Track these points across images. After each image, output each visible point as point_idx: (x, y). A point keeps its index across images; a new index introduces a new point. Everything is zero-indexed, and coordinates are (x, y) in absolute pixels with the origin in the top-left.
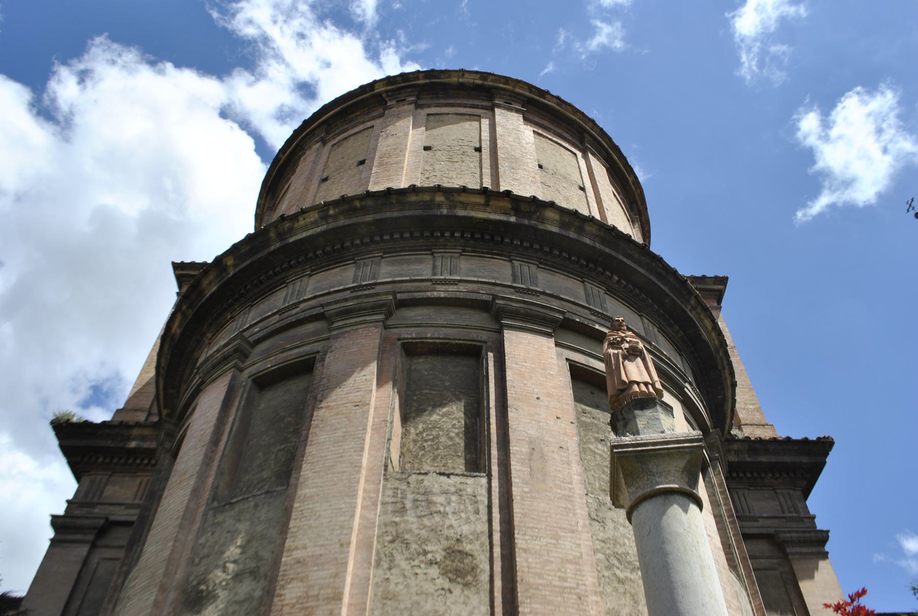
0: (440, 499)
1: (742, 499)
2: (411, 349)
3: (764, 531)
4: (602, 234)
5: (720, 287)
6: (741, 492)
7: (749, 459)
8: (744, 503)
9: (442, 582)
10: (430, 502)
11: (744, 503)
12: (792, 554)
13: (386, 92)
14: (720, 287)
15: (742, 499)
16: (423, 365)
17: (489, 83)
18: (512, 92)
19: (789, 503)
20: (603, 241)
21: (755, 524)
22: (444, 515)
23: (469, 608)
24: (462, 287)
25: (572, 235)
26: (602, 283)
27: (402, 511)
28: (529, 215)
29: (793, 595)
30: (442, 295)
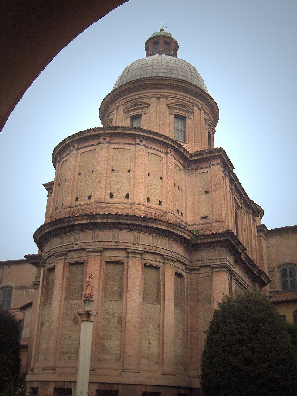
0: (73, 306)
2: (72, 264)
3: (208, 264)
9: (73, 324)
10: (72, 307)
13: (70, 142)
16: (74, 268)
17: (97, 133)
18: (105, 133)
20: (114, 219)
21: (206, 262)
22: (74, 309)
23: (76, 328)
24: (80, 245)
25: (105, 221)
26: (118, 228)
27: (67, 309)
28: (93, 219)
30: (76, 248)
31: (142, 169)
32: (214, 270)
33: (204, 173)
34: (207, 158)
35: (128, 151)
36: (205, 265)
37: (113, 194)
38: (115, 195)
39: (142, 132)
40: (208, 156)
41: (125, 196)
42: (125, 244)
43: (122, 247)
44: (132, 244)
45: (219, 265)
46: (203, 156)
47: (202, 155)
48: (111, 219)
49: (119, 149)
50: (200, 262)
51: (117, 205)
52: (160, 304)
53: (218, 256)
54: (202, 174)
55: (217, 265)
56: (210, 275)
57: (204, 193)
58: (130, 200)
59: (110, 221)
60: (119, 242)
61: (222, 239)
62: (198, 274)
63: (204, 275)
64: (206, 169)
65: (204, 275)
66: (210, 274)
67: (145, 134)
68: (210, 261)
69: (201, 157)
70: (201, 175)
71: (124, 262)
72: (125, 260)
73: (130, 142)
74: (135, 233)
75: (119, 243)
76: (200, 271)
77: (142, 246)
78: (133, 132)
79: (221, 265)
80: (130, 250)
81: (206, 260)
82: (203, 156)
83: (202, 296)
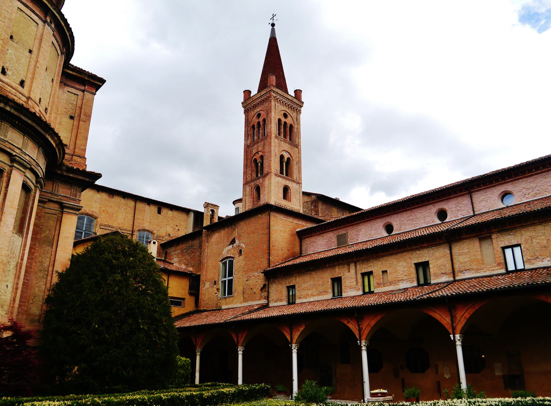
1: (57, 186)
3: (59, 200)
4: (16, 106)
5: (101, 84)
6: (58, 184)
7: (65, 174)
8: (57, 188)
11: (57, 188)
12: (65, 211)
14: (101, 84)
15: (57, 186)
19: (75, 192)
20: (15, 109)
29: (58, 225)
31: (45, 59)
32: (64, 210)
33: (73, 94)
34: (85, 80)
35: (35, 23)
36: (55, 200)
37: (6, 70)
38: (8, 73)
39: (57, 13)
40: (86, 78)
41: (20, 82)
42: (12, 146)
43: (9, 150)
44: (20, 151)
45: (74, 206)
46: (80, 76)
47: (79, 74)
48: (11, 107)
49: (24, 14)
50: (50, 195)
51: (10, 88)
52: (23, 237)
53: (73, 196)
54: (70, 94)
55: (72, 206)
56: (57, 214)
57: (68, 116)
58: (25, 91)
59: (8, 108)
60: (7, 141)
61: (87, 180)
62: (44, 207)
63: (50, 211)
64: (79, 91)
65: (50, 211)
66: (58, 212)
67: (59, 18)
68: (63, 198)
69: (78, 75)
70: (69, 94)
71: (5, 171)
72: (7, 168)
73: (39, 14)
74: (25, 138)
75: (7, 143)
76: (46, 206)
77: (29, 158)
78: (49, 6)
79: (76, 207)
80: (18, 158)
81: (57, 195)
82: (80, 76)
83: (43, 236)
